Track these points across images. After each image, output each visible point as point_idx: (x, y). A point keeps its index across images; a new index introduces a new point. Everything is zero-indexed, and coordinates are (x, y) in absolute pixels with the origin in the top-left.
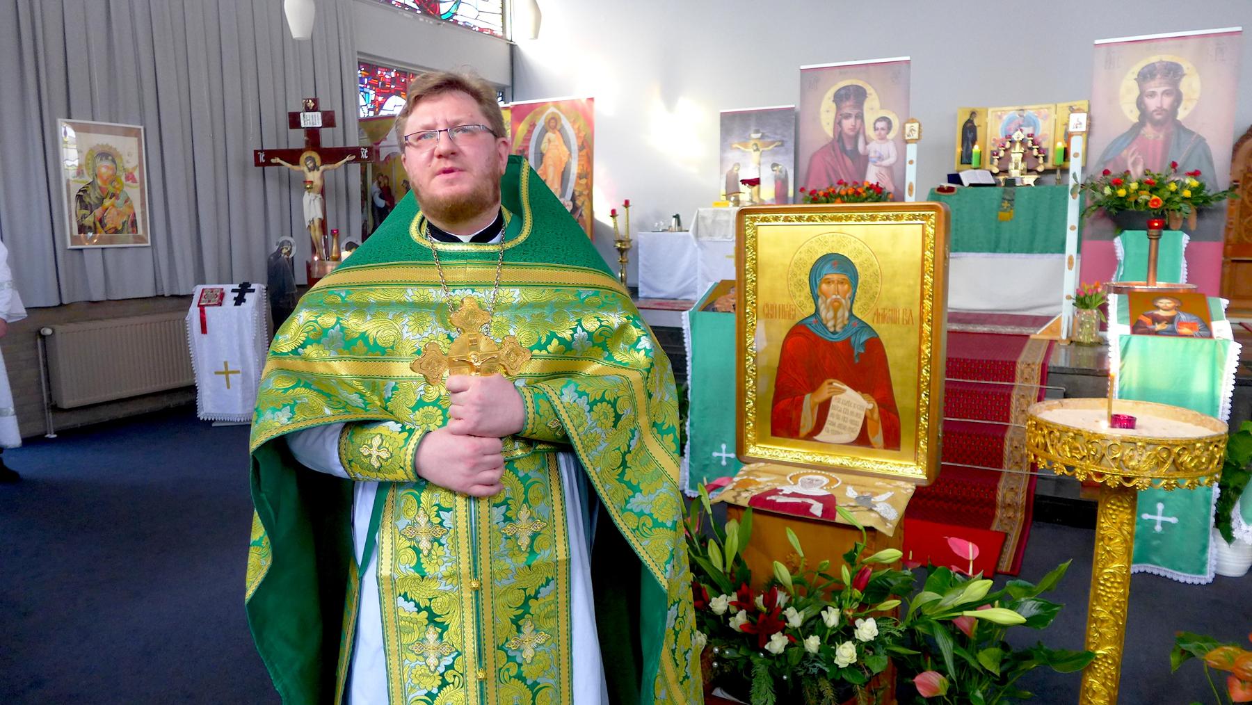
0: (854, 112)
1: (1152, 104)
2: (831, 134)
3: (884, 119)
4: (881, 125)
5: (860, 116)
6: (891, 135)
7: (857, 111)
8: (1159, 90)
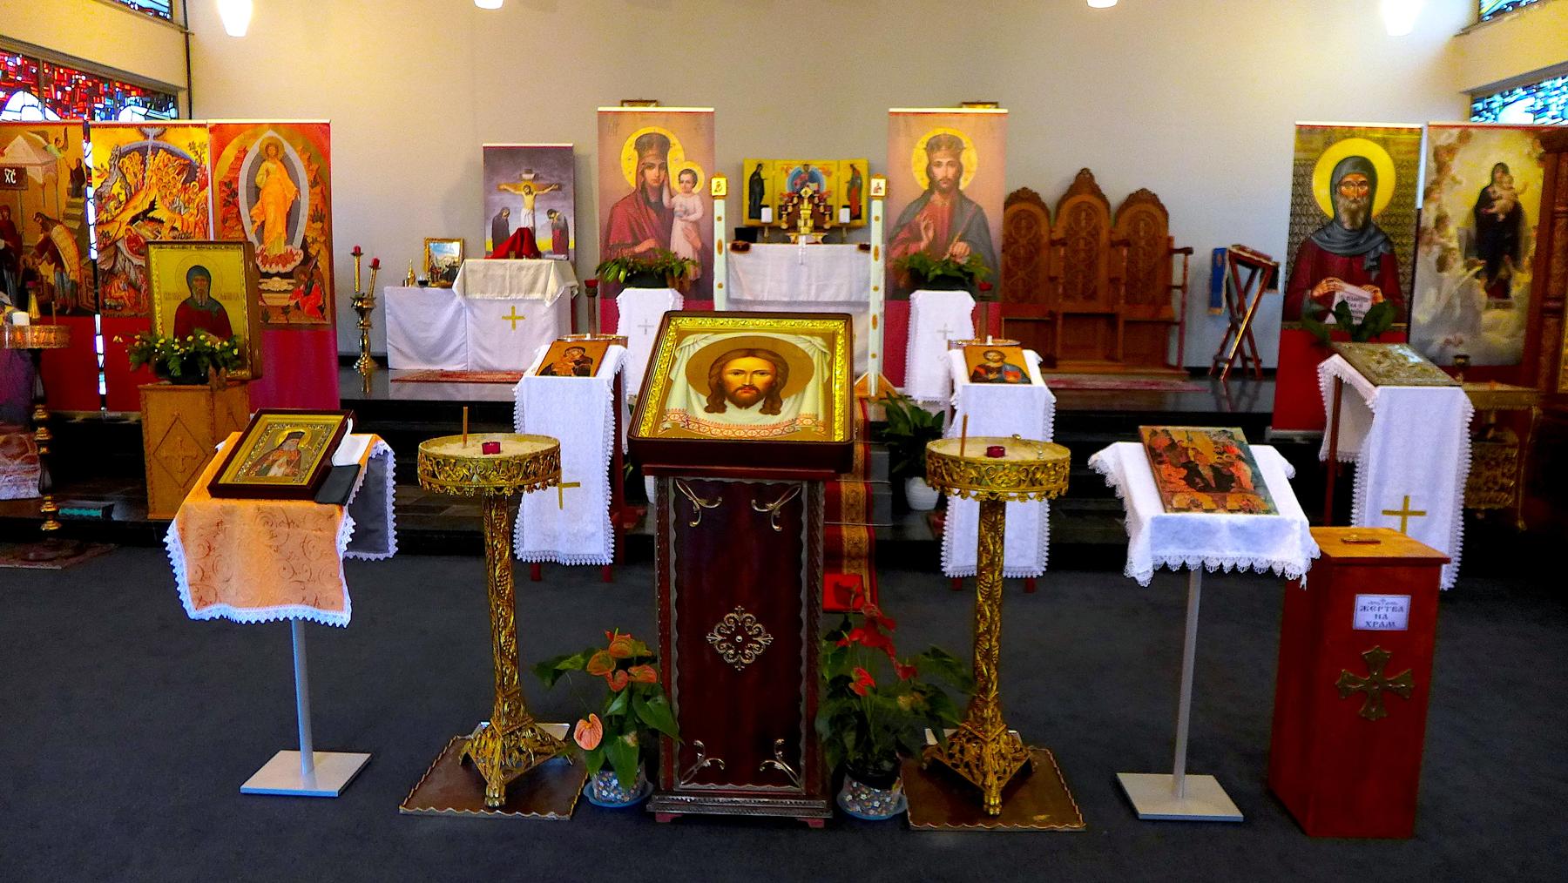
1: (939, 173)
2: (634, 185)
4: (685, 177)
6: (697, 189)
8: (945, 161)
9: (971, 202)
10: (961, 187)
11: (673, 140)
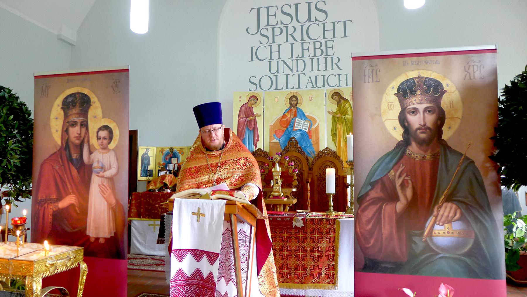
0: (79, 120)
1: (415, 121)
3: (106, 128)
4: (103, 134)
5: (85, 125)
6: (112, 146)
8: (421, 107)
9: (462, 155)
10: (444, 137)
11: (94, 98)
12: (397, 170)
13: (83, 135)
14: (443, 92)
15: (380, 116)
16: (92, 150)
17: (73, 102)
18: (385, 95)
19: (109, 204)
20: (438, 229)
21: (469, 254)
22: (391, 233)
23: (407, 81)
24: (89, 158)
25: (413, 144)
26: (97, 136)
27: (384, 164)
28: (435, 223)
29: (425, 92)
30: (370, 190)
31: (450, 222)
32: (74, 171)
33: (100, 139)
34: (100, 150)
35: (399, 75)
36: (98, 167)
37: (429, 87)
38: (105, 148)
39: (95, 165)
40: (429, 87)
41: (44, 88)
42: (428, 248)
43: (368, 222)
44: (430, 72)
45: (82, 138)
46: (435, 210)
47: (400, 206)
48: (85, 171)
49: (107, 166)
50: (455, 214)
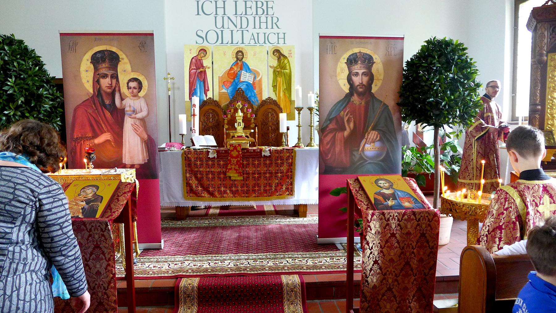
0: (110, 73)
1: (357, 80)
4: (132, 84)
5: (115, 77)
7: (113, 72)
8: (361, 72)
9: (382, 102)
10: (373, 91)
12: (345, 111)
13: (114, 85)
14: (374, 63)
15: (336, 76)
16: (123, 97)
17: (102, 57)
18: (339, 63)
19: (142, 139)
20: (367, 146)
21: (382, 161)
22: (341, 149)
23: (353, 54)
24: (121, 103)
25: (355, 95)
26: (128, 86)
27: (337, 107)
28: (366, 143)
29: (363, 62)
30: (329, 124)
31: (374, 142)
32: (108, 114)
33: (131, 88)
34: (131, 97)
35: (348, 50)
36: (131, 111)
37: (365, 59)
38: (135, 96)
39: (127, 109)
40: (365, 59)
41: (71, 44)
42: (361, 158)
43: (328, 144)
44: (366, 50)
45: (113, 88)
46: (366, 135)
47: (346, 133)
48: (119, 115)
49: (138, 110)
50: (377, 137)
